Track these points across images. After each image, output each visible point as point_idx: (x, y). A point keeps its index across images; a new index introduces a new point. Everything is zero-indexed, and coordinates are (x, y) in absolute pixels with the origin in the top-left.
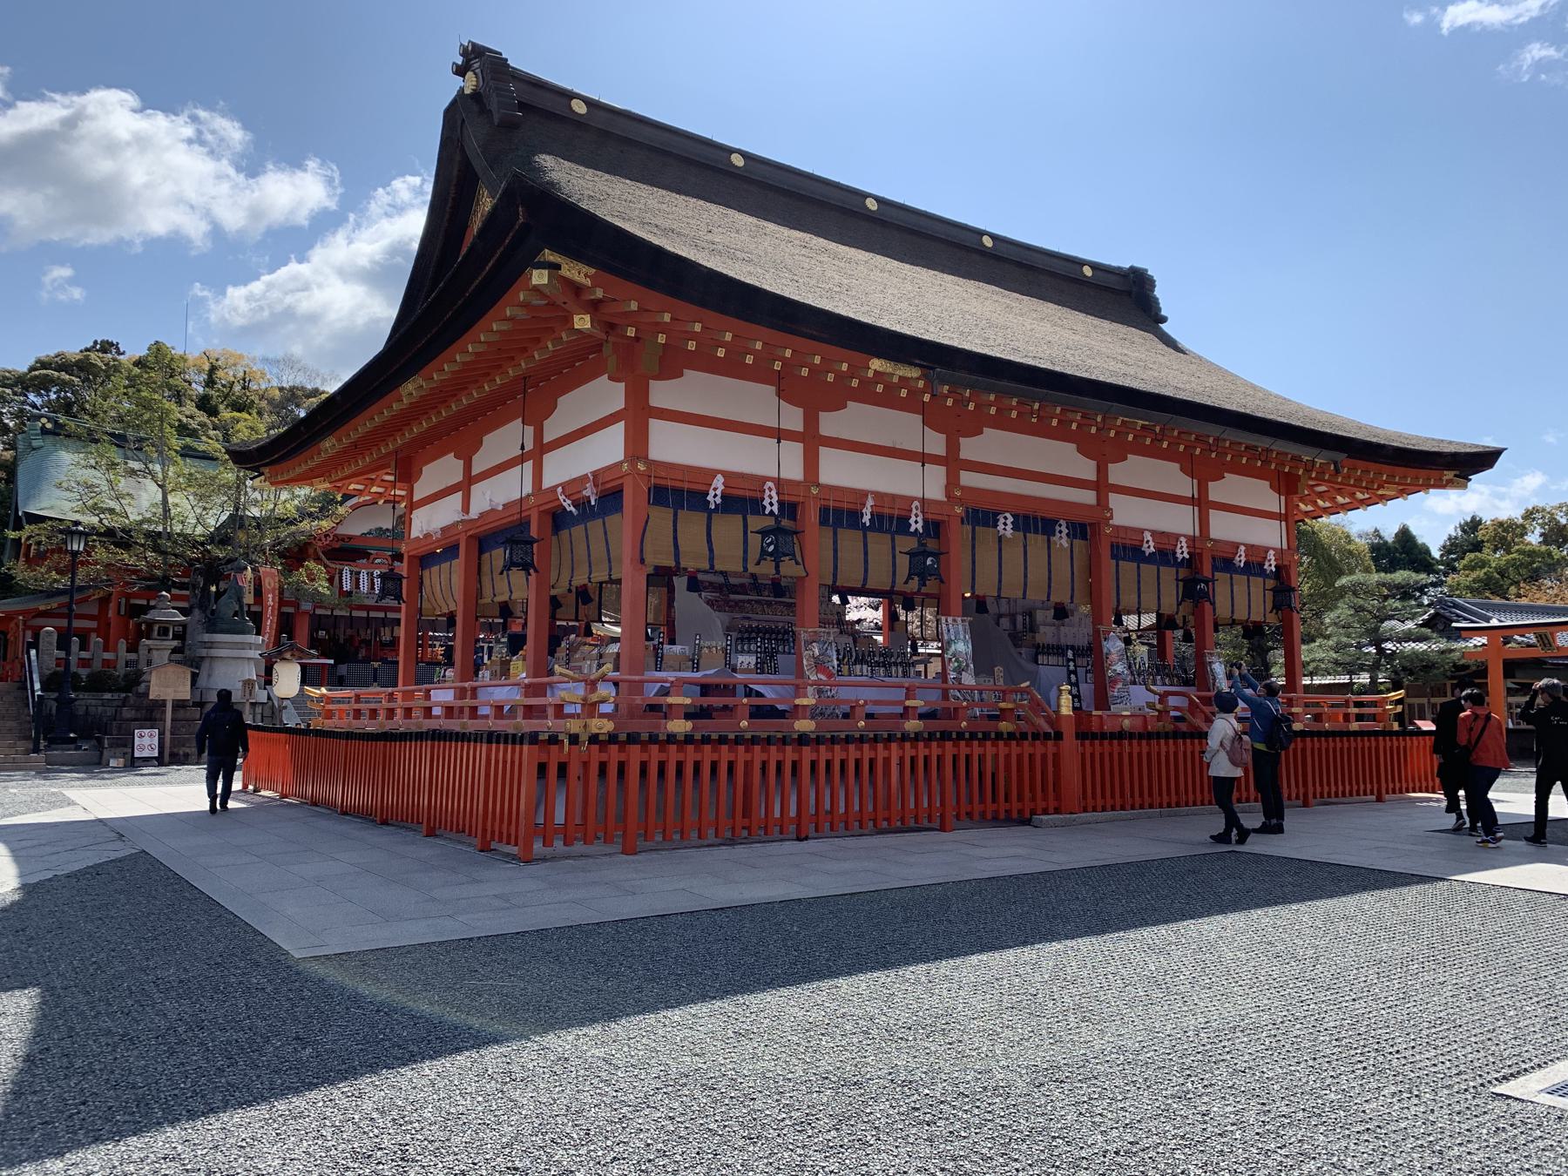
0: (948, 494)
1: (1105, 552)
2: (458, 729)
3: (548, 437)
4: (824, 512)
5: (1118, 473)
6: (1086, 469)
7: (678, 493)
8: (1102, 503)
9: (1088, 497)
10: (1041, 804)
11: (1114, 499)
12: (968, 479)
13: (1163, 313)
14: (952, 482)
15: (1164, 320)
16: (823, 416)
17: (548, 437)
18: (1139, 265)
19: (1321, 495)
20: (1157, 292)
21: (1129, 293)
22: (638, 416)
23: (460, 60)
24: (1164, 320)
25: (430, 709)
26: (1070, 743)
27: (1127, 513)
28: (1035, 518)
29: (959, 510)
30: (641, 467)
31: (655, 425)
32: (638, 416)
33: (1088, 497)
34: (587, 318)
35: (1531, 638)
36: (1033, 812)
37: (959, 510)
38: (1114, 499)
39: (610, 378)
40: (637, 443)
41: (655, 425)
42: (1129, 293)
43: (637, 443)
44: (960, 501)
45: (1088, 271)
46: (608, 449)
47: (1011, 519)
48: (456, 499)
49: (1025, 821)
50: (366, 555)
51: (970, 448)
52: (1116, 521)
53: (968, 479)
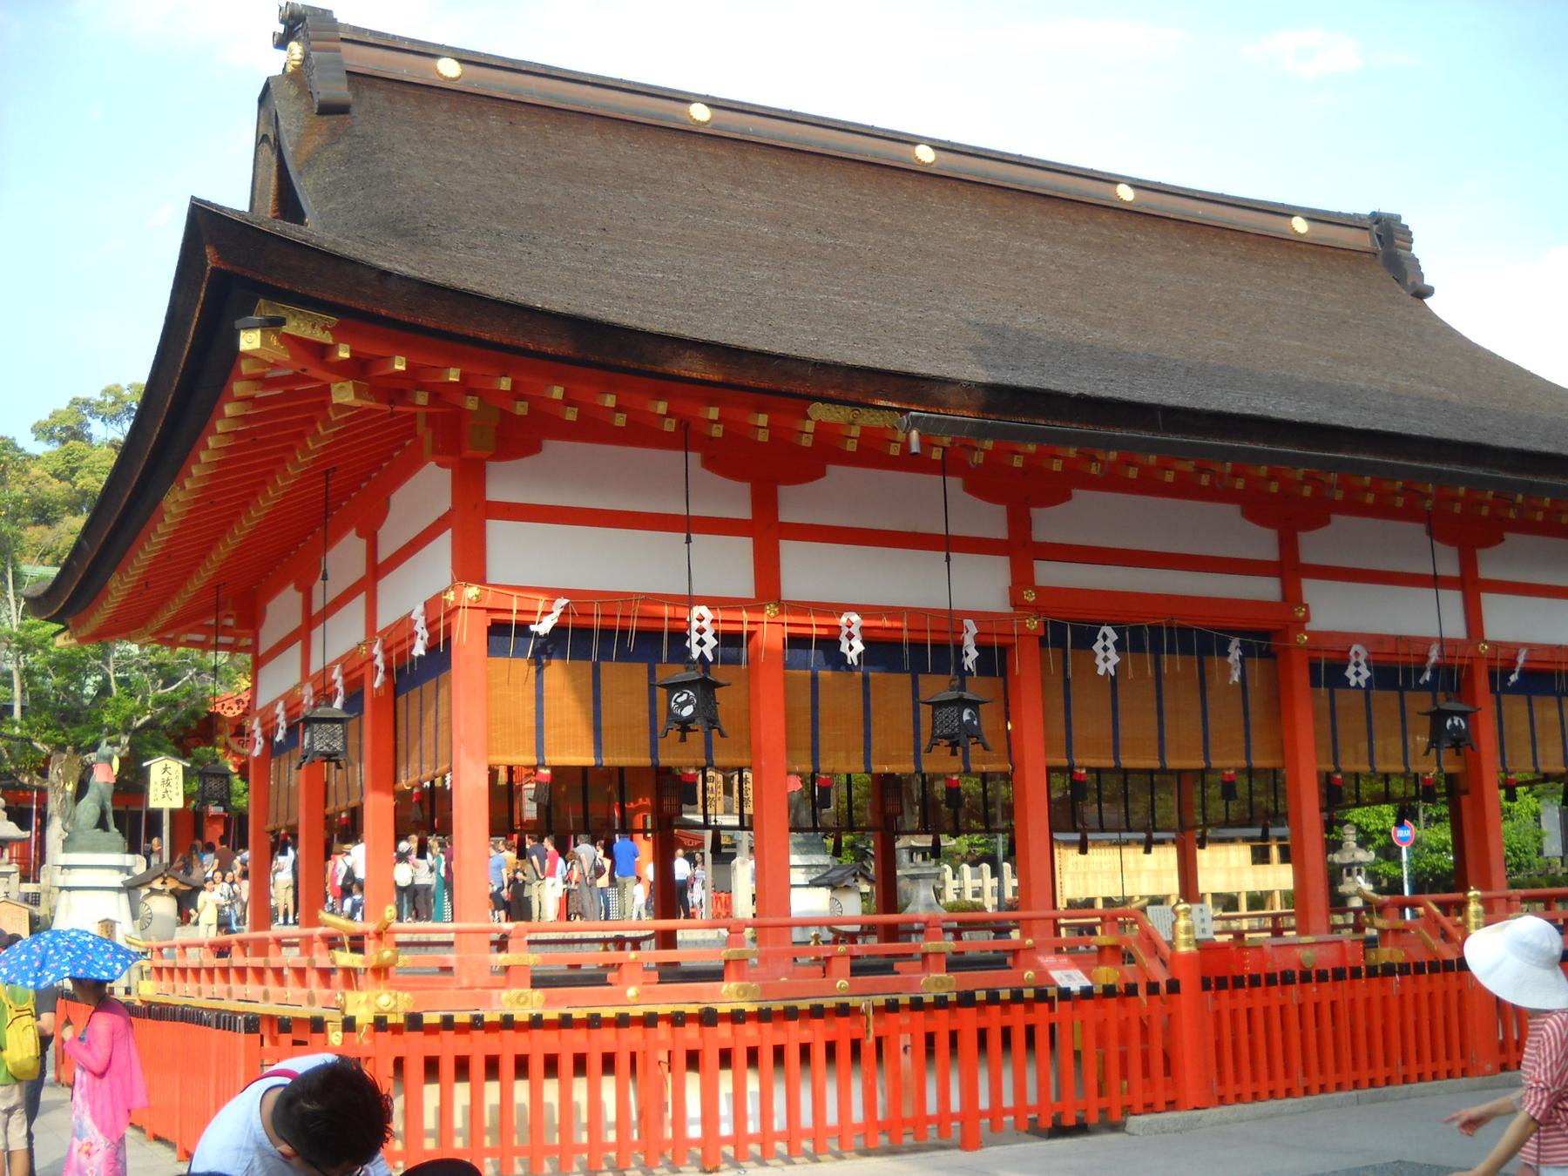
0: (1017, 602)
1: (1301, 678)
5: (1314, 547)
6: (1262, 543)
8: (1292, 596)
9: (1266, 589)
11: (1312, 590)
12: (1049, 574)
13: (1427, 282)
16: (786, 493)
18: (1386, 208)
27: (1332, 610)
28: (1170, 629)
29: (1033, 624)
31: (497, 531)
33: (1266, 589)
36: (1129, 1110)
37: (1033, 624)
38: (1312, 590)
41: (497, 531)
44: (1036, 609)
47: (1113, 636)
49: (1117, 1127)
51: (1048, 525)
53: (1049, 574)
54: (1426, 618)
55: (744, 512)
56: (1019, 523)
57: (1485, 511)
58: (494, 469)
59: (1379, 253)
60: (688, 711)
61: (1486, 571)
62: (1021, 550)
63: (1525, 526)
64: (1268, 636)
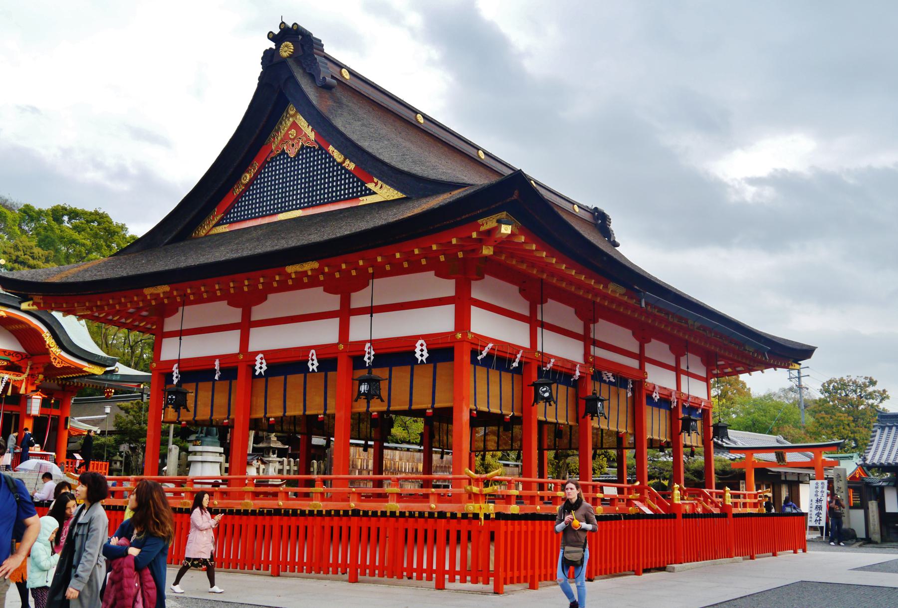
8: (642, 367)
11: (648, 367)
14: (587, 354)
15: (618, 245)
19: (718, 367)
22: (462, 304)
23: (277, 31)
24: (618, 245)
32: (462, 304)
33: (634, 364)
34: (492, 249)
35: (772, 457)
38: (648, 367)
39: (436, 275)
40: (462, 320)
43: (462, 320)
48: (236, 335)
55: (526, 312)
58: (473, 282)
60: (547, 395)
62: (588, 341)
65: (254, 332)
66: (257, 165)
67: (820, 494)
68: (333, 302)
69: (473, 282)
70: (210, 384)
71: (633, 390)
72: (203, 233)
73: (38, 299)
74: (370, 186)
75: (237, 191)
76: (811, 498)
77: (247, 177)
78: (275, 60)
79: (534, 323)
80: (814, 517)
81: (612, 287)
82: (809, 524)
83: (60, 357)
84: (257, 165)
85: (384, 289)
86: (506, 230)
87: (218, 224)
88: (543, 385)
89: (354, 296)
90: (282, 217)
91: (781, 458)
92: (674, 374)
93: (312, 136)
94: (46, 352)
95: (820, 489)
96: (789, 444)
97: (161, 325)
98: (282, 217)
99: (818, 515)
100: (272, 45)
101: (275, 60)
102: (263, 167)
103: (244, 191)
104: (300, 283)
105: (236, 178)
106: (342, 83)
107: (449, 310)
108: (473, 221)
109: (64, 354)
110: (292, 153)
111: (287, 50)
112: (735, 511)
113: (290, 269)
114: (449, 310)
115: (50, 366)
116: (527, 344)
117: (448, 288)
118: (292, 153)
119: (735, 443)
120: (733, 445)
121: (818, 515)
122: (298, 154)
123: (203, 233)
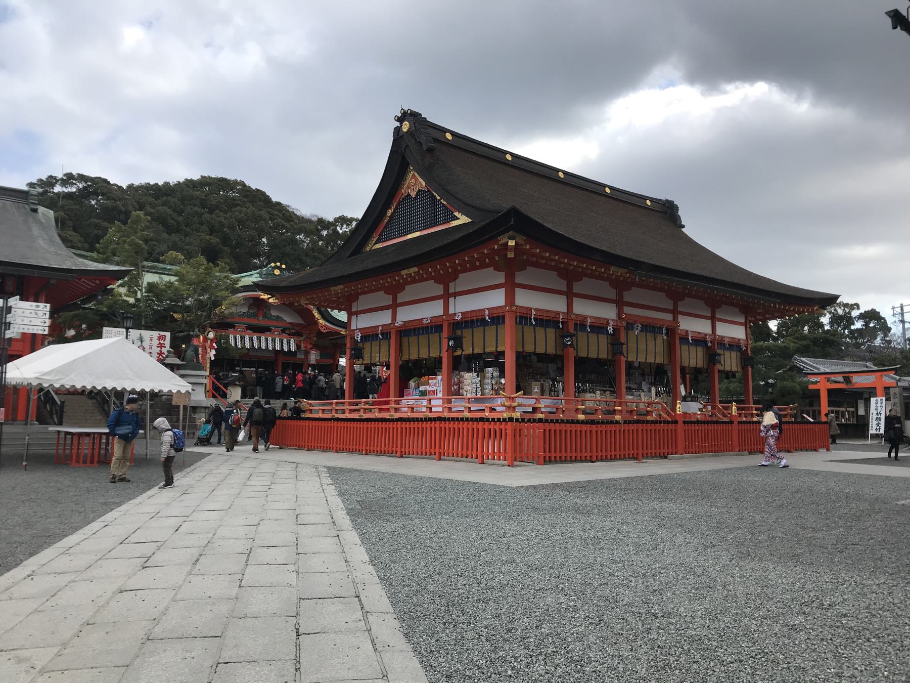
2: (388, 417)
3: (451, 291)
4: (576, 324)
6: (669, 305)
7: (523, 318)
8: (675, 319)
10: (671, 450)
11: (681, 318)
12: (627, 310)
15: (683, 227)
17: (451, 291)
19: (759, 314)
20: (680, 213)
21: (666, 213)
22: (510, 287)
23: (400, 115)
24: (683, 227)
25: (431, 408)
26: (680, 426)
30: (514, 308)
31: (518, 291)
33: (669, 317)
35: (841, 379)
38: (681, 318)
40: (510, 298)
41: (518, 291)
42: (666, 213)
45: (648, 202)
46: (495, 299)
49: (666, 458)
50: (234, 327)
52: (681, 328)
54: (556, 305)
56: (620, 295)
57: (562, 266)
58: (517, 273)
59: (667, 212)
61: (717, 316)
62: (620, 303)
63: (690, 295)
64: (672, 332)
65: (400, 310)
66: (395, 204)
67: (879, 408)
68: (439, 290)
69: (517, 273)
70: (378, 342)
71: (667, 334)
72: (368, 249)
73: (278, 296)
74: (456, 214)
75: (386, 221)
76: (878, 410)
77: (390, 212)
78: (401, 134)
79: (570, 295)
80: (875, 427)
81: (613, 269)
82: (871, 432)
83: (325, 326)
84: (395, 204)
85: (464, 281)
86: (511, 243)
87: (376, 243)
88: (567, 337)
89: (452, 285)
90: (410, 236)
91: (847, 380)
92: (709, 322)
93: (424, 183)
94: (316, 322)
95: (879, 405)
96: (876, 368)
97: (351, 307)
98: (410, 236)
99: (878, 424)
100: (398, 124)
101: (401, 134)
102: (398, 205)
103: (389, 221)
104: (413, 280)
105: (383, 213)
106: (446, 143)
107: (501, 292)
108: (494, 238)
109: (327, 324)
110: (413, 194)
111: (406, 127)
112: (740, 419)
113: (404, 272)
114: (501, 292)
115: (319, 332)
116: (565, 311)
117: (501, 278)
118: (413, 194)
119: (818, 369)
120: (817, 371)
121: (878, 424)
122: (417, 195)
123: (368, 249)
